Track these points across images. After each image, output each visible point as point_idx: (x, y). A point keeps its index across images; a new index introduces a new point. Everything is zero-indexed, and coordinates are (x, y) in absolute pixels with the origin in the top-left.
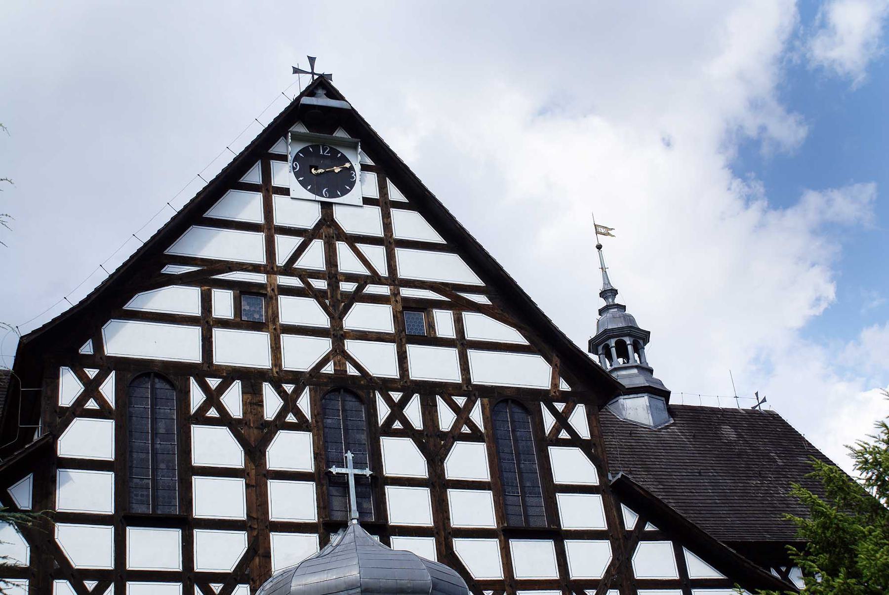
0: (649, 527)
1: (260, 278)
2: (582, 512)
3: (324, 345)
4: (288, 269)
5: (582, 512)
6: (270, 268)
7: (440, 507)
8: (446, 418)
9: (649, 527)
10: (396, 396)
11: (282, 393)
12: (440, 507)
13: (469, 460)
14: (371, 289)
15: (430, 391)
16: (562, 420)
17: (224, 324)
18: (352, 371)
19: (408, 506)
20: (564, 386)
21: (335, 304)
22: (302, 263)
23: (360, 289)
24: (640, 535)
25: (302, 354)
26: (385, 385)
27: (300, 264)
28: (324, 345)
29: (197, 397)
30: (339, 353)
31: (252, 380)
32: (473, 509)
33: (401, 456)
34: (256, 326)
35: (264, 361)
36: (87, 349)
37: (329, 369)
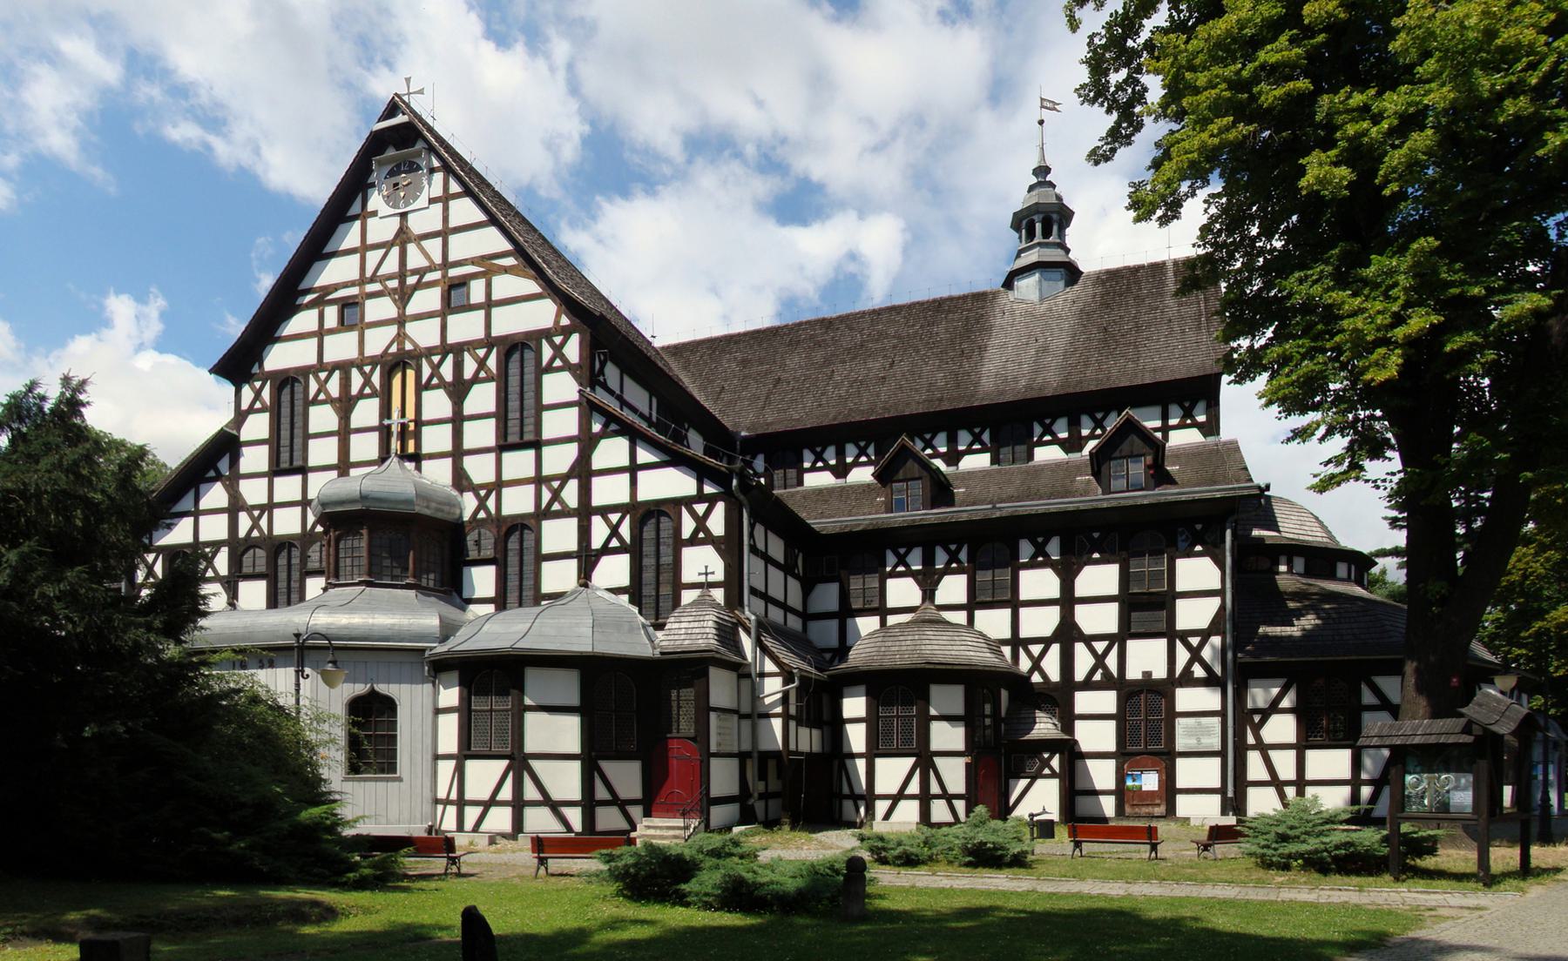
1: (354, 291)
2: (561, 424)
3: (392, 330)
4: (372, 280)
5: (561, 424)
6: (362, 281)
7: (458, 436)
10: (436, 359)
11: (363, 373)
12: (458, 436)
13: (482, 398)
14: (429, 277)
15: (458, 350)
16: (558, 350)
17: (332, 331)
18: (408, 346)
19: (436, 439)
20: (565, 321)
21: (402, 298)
22: (382, 271)
23: (419, 280)
25: (378, 341)
26: (430, 352)
27: (382, 271)
28: (392, 330)
30: (401, 337)
31: (344, 367)
32: (481, 434)
33: (437, 404)
34: (351, 328)
35: (352, 353)
37: (394, 349)
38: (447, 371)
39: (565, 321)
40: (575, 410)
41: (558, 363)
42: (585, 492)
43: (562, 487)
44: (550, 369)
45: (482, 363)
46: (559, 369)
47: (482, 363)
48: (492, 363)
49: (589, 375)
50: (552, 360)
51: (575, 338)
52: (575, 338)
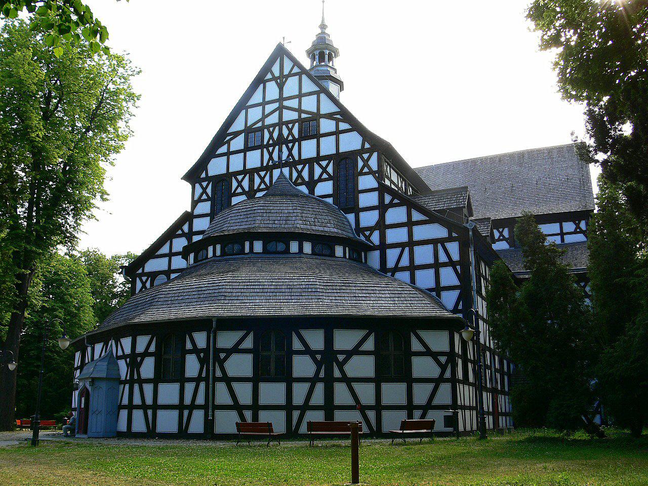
0: (396, 201)
5: (368, 200)
8: (318, 171)
9: (396, 201)
20: (367, 146)
24: (392, 205)
29: (235, 184)
36: (203, 175)
38: (305, 174)
39: (367, 146)
40: (376, 194)
41: (366, 170)
42: (383, 237)
43: (371, 235)
44: (362, 173)
45: (324, 170)
46: (366, 174)
47: (324, 170)
48: (330, 169)
49: (379, 175)
50: (363, 168)
51: (375, 155)
52: (375, 155)
